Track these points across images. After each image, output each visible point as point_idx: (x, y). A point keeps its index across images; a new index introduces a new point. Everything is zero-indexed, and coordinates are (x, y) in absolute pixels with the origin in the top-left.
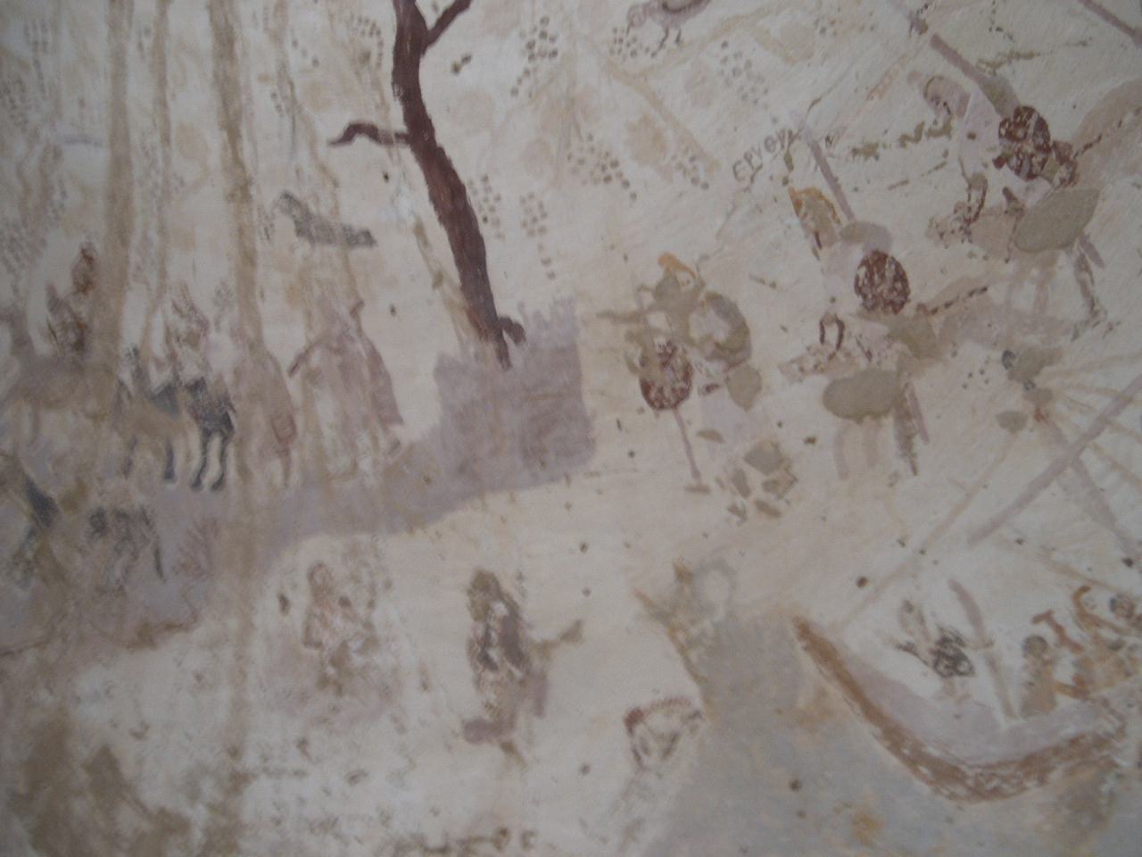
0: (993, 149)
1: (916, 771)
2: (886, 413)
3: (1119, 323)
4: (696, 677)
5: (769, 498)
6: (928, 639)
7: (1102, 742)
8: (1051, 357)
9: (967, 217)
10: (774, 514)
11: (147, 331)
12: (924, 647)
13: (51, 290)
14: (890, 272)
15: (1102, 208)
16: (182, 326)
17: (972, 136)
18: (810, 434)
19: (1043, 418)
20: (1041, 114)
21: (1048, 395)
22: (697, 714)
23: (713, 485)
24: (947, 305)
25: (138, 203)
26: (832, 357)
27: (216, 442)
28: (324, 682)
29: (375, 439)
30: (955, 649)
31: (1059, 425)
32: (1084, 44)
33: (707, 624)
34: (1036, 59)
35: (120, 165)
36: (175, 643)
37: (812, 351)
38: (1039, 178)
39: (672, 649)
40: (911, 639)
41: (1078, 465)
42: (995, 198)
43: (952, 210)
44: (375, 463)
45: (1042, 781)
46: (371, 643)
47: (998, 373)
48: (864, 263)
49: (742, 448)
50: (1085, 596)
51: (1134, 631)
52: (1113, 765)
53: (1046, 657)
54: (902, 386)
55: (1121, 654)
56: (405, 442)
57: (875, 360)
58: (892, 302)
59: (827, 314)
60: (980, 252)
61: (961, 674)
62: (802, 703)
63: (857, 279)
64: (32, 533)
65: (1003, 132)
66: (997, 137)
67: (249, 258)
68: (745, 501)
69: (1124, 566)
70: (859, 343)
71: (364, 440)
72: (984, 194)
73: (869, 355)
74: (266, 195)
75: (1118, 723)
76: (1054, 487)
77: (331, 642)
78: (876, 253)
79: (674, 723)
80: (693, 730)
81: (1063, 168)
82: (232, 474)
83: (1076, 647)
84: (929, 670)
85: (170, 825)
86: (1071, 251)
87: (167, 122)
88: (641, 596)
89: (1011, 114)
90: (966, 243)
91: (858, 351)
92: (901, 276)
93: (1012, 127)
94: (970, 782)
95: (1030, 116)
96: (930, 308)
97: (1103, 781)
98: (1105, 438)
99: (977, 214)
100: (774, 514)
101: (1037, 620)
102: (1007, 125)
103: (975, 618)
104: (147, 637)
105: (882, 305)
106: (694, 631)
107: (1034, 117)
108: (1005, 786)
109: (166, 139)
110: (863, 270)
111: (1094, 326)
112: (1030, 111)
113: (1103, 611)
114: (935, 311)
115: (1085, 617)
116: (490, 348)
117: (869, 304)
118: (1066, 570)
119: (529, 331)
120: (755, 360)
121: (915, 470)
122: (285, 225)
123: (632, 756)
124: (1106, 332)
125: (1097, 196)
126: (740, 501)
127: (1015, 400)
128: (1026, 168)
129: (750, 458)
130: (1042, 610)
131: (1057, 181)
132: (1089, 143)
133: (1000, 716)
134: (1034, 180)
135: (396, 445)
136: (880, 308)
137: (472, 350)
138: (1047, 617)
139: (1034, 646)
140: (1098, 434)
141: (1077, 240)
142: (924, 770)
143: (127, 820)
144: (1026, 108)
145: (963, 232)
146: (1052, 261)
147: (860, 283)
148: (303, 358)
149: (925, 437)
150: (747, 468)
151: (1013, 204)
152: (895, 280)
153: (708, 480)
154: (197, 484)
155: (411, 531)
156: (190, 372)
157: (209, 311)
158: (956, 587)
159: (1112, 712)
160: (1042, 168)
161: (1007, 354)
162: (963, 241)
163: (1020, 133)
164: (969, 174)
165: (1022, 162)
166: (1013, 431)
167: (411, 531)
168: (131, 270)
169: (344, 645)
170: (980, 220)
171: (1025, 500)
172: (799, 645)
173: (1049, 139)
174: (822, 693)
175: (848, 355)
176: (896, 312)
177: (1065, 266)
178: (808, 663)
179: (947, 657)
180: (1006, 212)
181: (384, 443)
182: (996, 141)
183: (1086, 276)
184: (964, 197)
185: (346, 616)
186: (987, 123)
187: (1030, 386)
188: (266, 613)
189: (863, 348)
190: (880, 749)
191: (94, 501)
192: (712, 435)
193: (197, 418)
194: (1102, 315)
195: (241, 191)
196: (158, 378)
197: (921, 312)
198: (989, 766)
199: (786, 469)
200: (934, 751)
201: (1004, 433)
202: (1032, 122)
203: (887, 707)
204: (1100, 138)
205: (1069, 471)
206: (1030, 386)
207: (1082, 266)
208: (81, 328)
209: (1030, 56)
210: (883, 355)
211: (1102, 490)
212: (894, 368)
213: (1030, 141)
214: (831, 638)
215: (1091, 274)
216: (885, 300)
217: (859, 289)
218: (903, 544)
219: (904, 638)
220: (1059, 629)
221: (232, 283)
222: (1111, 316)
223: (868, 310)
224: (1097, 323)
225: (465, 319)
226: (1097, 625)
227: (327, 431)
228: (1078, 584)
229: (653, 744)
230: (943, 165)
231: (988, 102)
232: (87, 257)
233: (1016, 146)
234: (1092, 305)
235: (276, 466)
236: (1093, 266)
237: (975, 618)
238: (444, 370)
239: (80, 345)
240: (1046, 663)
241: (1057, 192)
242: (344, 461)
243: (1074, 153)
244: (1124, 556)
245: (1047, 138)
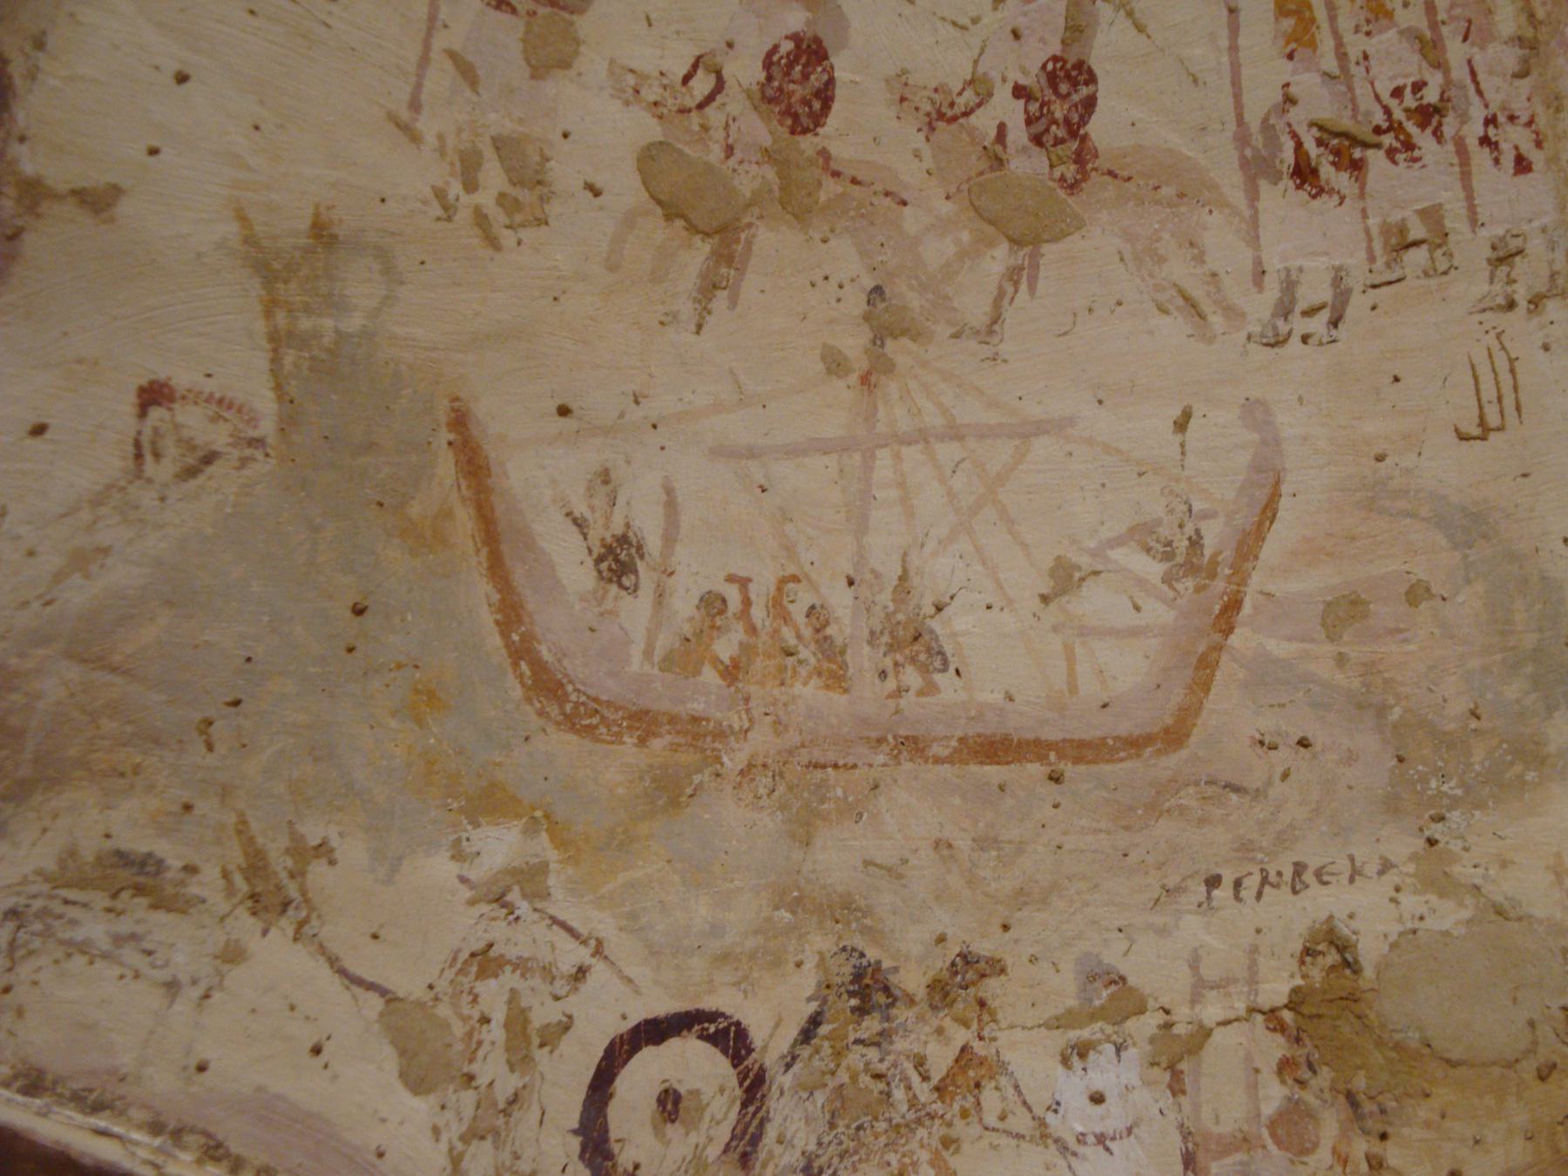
0: (1025, 72)
1: (516, 665)
2: (707, 234)
3: (1005, 361)
4: (278, 387)
5: (498, 216)
6: (607, 528)
7: (720, 734)
8: (917, 335)
9: (944, 110)
10: (493, 243)
12: (595, 534)
14: (817, 79)
15: (1073, 243)
17: (1016, 34)
18: (599, 182)
19: (869, 385)
20: (1098, 95)
21: (889, 367)
22: (257, 442)
23: (431, 139)
24: (854, 181)
26: (684, 111)
30: (629, 555)
31: (881, 408)
32: (1195, 81)
33: (328, 323)
34: (1144, 37)
37: (665, 81)
38: (1044, 150)
39: (260, 326)
40: (588, 514)
41: (869, 457)
42: (985, 122)
43: (933, 84)
45: (642, 742)
47: (856, 302)
48: (796, 38)
49: (498, 121)
50: (791, 585)
51: (813, 647)
52: (718, 760)
53: (718, 621)
54: (745, 221)
55: (790, 661)
57: (732, 162)
58: (796, 117)
59: (713, 53)
60: (928, 162)
61: (621, 586)
62: (415, 510)
63: (775, 48)
65: (1050, 66)
66: (1040, 65)
68: (462, 193)
69: (844, 582)
70: (727, 126)
72: (979, 105)
73: (729, 150)
75: (746, 725)
76: (832, 460)
78: (817, 40)
79: (218, 437)
80: (244, 462)
81: (1073, 167)
83: (752, 630)
84: (590, 562)
86: (1016, 252)
88: (242, 218)
89: (1072, 60)
90: (921, 136)
91: (719, 134)
92: (825, 96)
93: (1062, 74)
94: (568, 707)
95: (1086, 83)
96: (834, 166)
97: (699, 771)
98: (912, 453)
99: (954, 119)
100: (493, 243)
101: (731, 579)
102: (1059, 65)
103: (670, 537)
105: (783, 107)
106: (305, 324)
107: (1092, 88)
108: (603, 729)
110: (787, 46)
111: (981, 342)
112: (1092, 79)
113: (798, 611)
114: (836, 174)
115: (778, 607)
117: (769, 92)
118: (790, 549)
120: (585, 25)
121: (699, 327)
123: (131, 449)
124: (988, 359)
125: (1080, 228)
126: (455, 189)
127: (853, 343)
128: (1039, 127)
129: (499, 144)
130: (743, 574)
131: (1057, 174)
132: (1117, 172)
133: (636, 652)
134: (1038, 149)
136: (777, 109)
138: (744, 583)
139: (713, 604)
140: (909, 444)
141: (1031, 247)
142: (524, 666)
144: (1090, 72)
145: (927, 119)
146: (991, 244)
147: (775, 58)
149: (733, 302)
150: (489, 152)
151: (999, 148)
152: (817, 94)
153: (427, 126)
158: (669, 491)
159: (748, 711)
160: (1054, 145)
161: (878, 290)
162: (919, 130)
163: (1064, 88)
164: (981, 69)
165: (1042, 115)
166: (829, 371)
170: (954, 126)
171: (793, 452)
172: (445, 435)
173: (1085, 124)
174: (447, 514)
175: (705, 128)
176: (793, 132)
177: (999, 258)
178: (446, 466)
179: (617, 560)
180: (985, 148)
182: (1035, 68)
183: (1010, 289)
184: (957, 87)
186: (1042, 40)
187: (878, 342)
189: (728, 136)
190: (487, 619)
192: (467, 72)
194: (996, 340)
197: (821, 160)
198: (596, 700)
199: (541, 198)
200: (546, 655)
201: (820, 366)
202: (1085, 91)
203: (518, 574)
204: (1129, 179)
205: (857, 457)
206: (878, 342)
207: (1013, 276)
209: (1140, 28)
210: (746, 166)
211: (875, 498)
212: (748, 195)
213: (1066, 107)
214: (491, 452)
215: (1016, 291)
216: (790, 106)
217: (768, 63)
218: (637, 402)
219: (581, 509)
220: (747, 602)
222: (1006, 349)
223: (763, 97)
224: (987, 343)
226: (785, 622)
228: (792, 570)
229: (171, 449)
230: (963, 28)
231: (1061, 21)
233: (1049, 94)
234: (994, 322)
236: (1024, 287)
237: (670, 537)
240: (712, 627)
241: (1051, 184)
243: (1095, 165)
244: (851, 573)
245: (1084, 121)
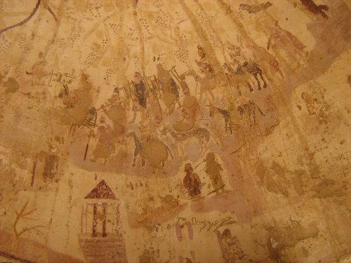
11: (225, 57)
13: (196, 61)
16: (234, 52)
25: (205, 29)
27: (258, 76)
28: (321, 122)
29: (300, 54)
35: (194, 22)
36: (276, 129)
44: (304, 60)
46: (328, 107)
56: (309, 52)
64: (226, 120)
67: (240, 26)
71: (298, 56)
74: (236, 8)
77: (318, 112)
82: (267, 82)
85: (300, 174)
87: (200, 4)
104: (268, 132)
109: (202, 9)
116: (320, 15)
119: (329, 6)
122: (245, 12)
135: (307, 53)
137: (315, 18)
143: (288, 176)
148: (269, 43)
154: (260, 89)
155: (324, 73)
156: (242, 62)
157: (238, 45)
167: (324, 73)
168: (213, 45)
169: (321, 111)
181: (304, 55)
185: (318, 103)
188: (297, 113)
191: (237, 106)
193: (250, 72)
195: (229, 10)
196: (235, 68)
208: (209, 66)
221: (240, 35)
225: (308, 12)
227: (286, 59)
232: (200, 48)
235: (278, 74)
238: (310, 28)
239: (211, 70)
242: (295, 64)
